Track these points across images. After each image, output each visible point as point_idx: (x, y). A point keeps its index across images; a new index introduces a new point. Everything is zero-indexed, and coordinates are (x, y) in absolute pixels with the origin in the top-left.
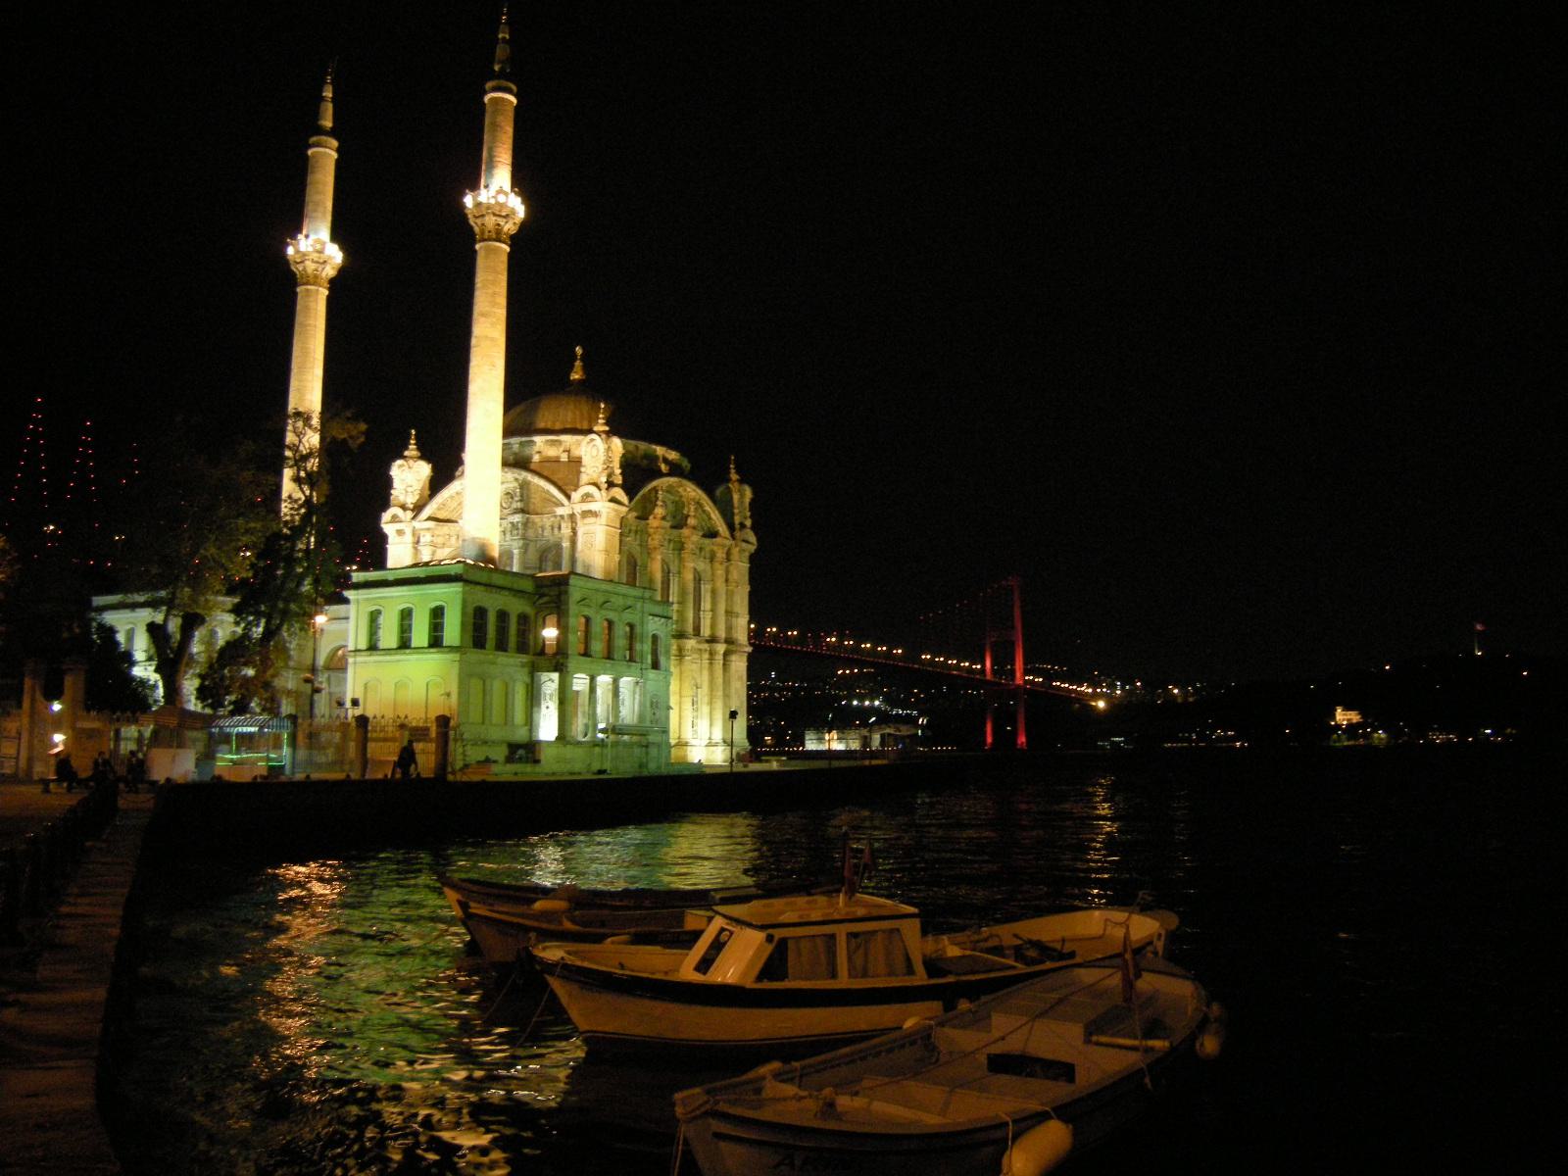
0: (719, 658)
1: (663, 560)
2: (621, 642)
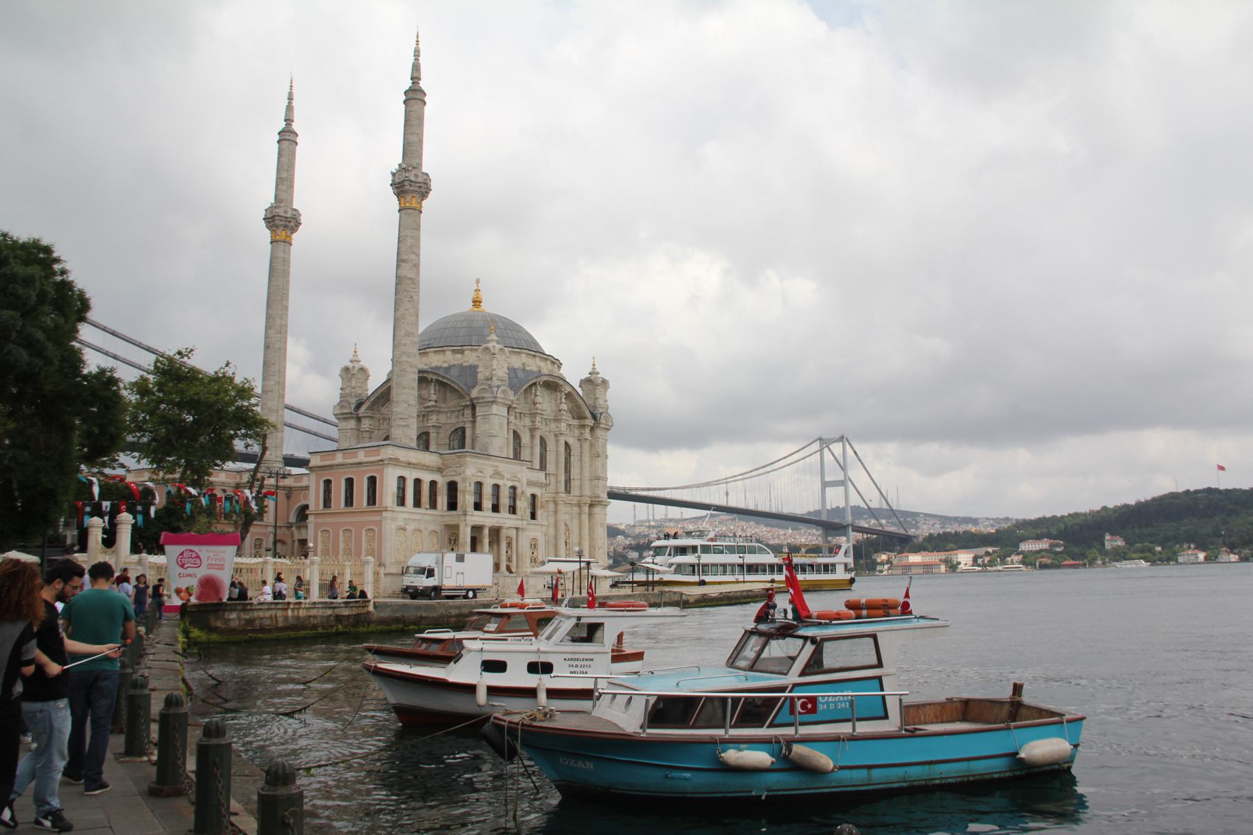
0: (586, 509)
1: (541, 437)
2: (505, 501)
